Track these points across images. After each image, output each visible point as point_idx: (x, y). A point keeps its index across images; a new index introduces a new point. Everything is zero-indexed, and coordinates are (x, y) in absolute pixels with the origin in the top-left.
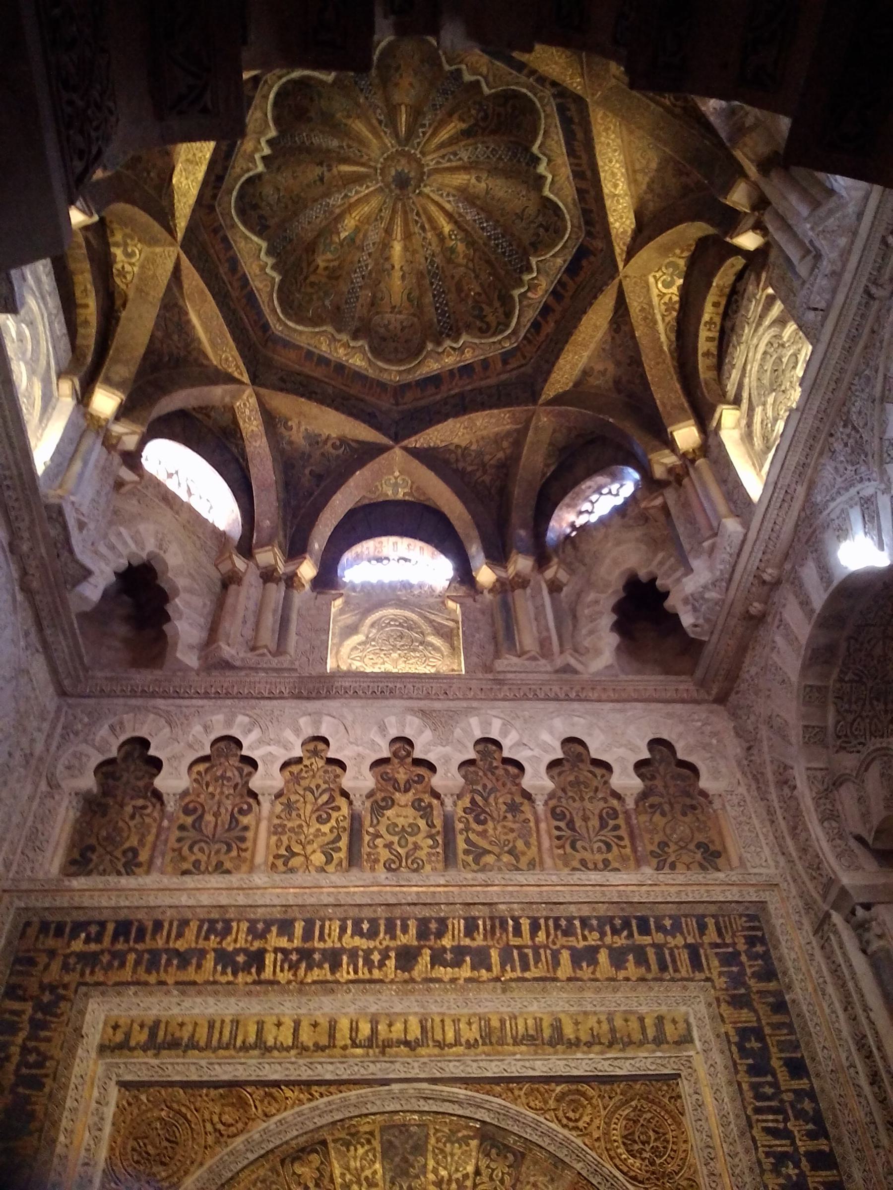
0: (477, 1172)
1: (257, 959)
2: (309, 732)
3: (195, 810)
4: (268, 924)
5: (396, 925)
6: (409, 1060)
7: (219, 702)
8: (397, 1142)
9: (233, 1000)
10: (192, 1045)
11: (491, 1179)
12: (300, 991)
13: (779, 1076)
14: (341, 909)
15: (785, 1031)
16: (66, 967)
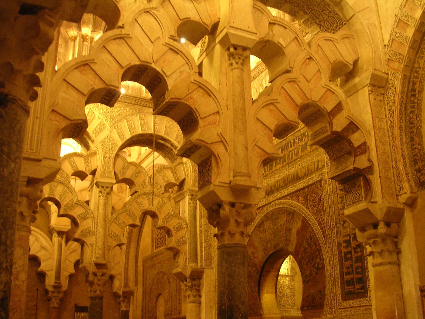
0: (286, 221)
6: (273, 195)
8: (274, 217)
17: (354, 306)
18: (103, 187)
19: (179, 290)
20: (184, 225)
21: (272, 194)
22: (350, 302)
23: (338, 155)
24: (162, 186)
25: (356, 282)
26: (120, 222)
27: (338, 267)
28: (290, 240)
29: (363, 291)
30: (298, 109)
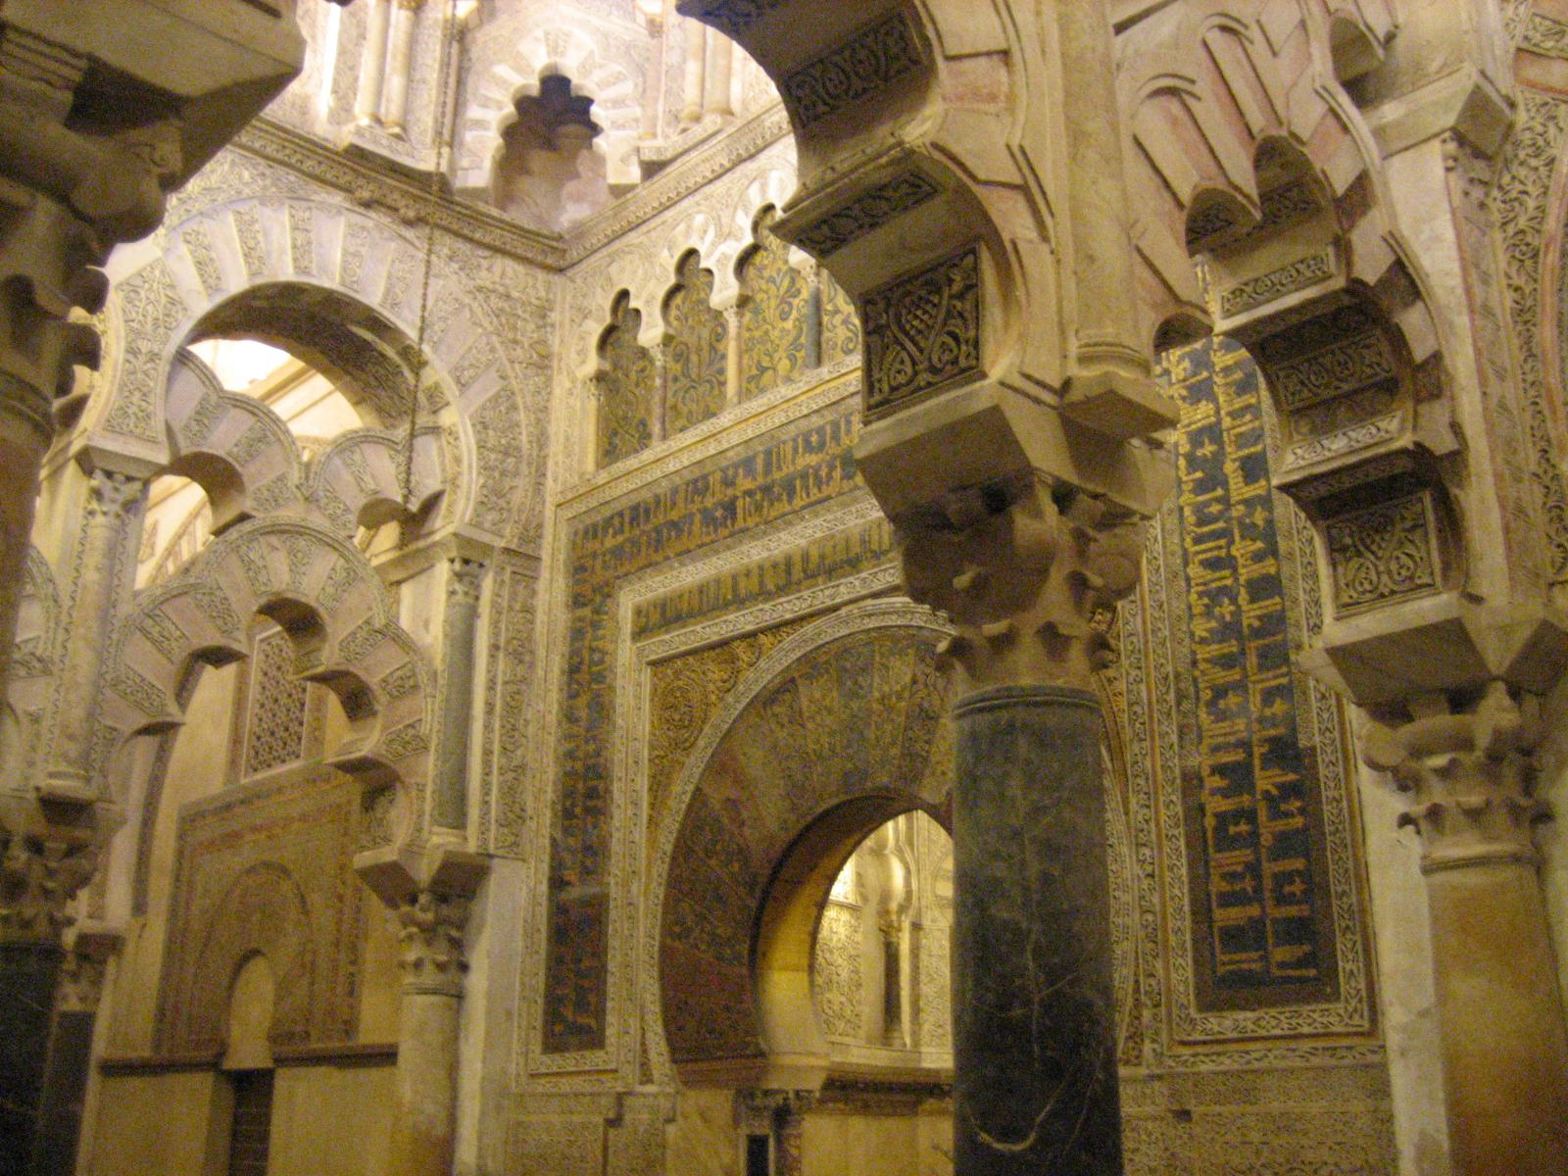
0: (914, 682)
1: (730, 508)
2: (757, 204)
3: (681, 355)
4: (736, 466)
5: (839, 428)
6: (851, 579)
7: (678, 208)
8: (848, 665)
9: (714, 559)
10: (691, 615)
11: (926, 686)
12: (765, 533)
13: (1232, 485)
14: (792, 427)
15: (1248, 417)
16: (605, 566)
17: (1264, 1033)
18: (109, 475)
19: (350, 944)
20: (423, 678)
21: (850, 575)
22: (1245, 1018)
23: (1326, 394)
24: (353, 508)
25: (1276, 933)
26: (166, 634)
27: (1184, 871)
28: (926, 759)
29: (1312, 972)
30: (1253, 151)
